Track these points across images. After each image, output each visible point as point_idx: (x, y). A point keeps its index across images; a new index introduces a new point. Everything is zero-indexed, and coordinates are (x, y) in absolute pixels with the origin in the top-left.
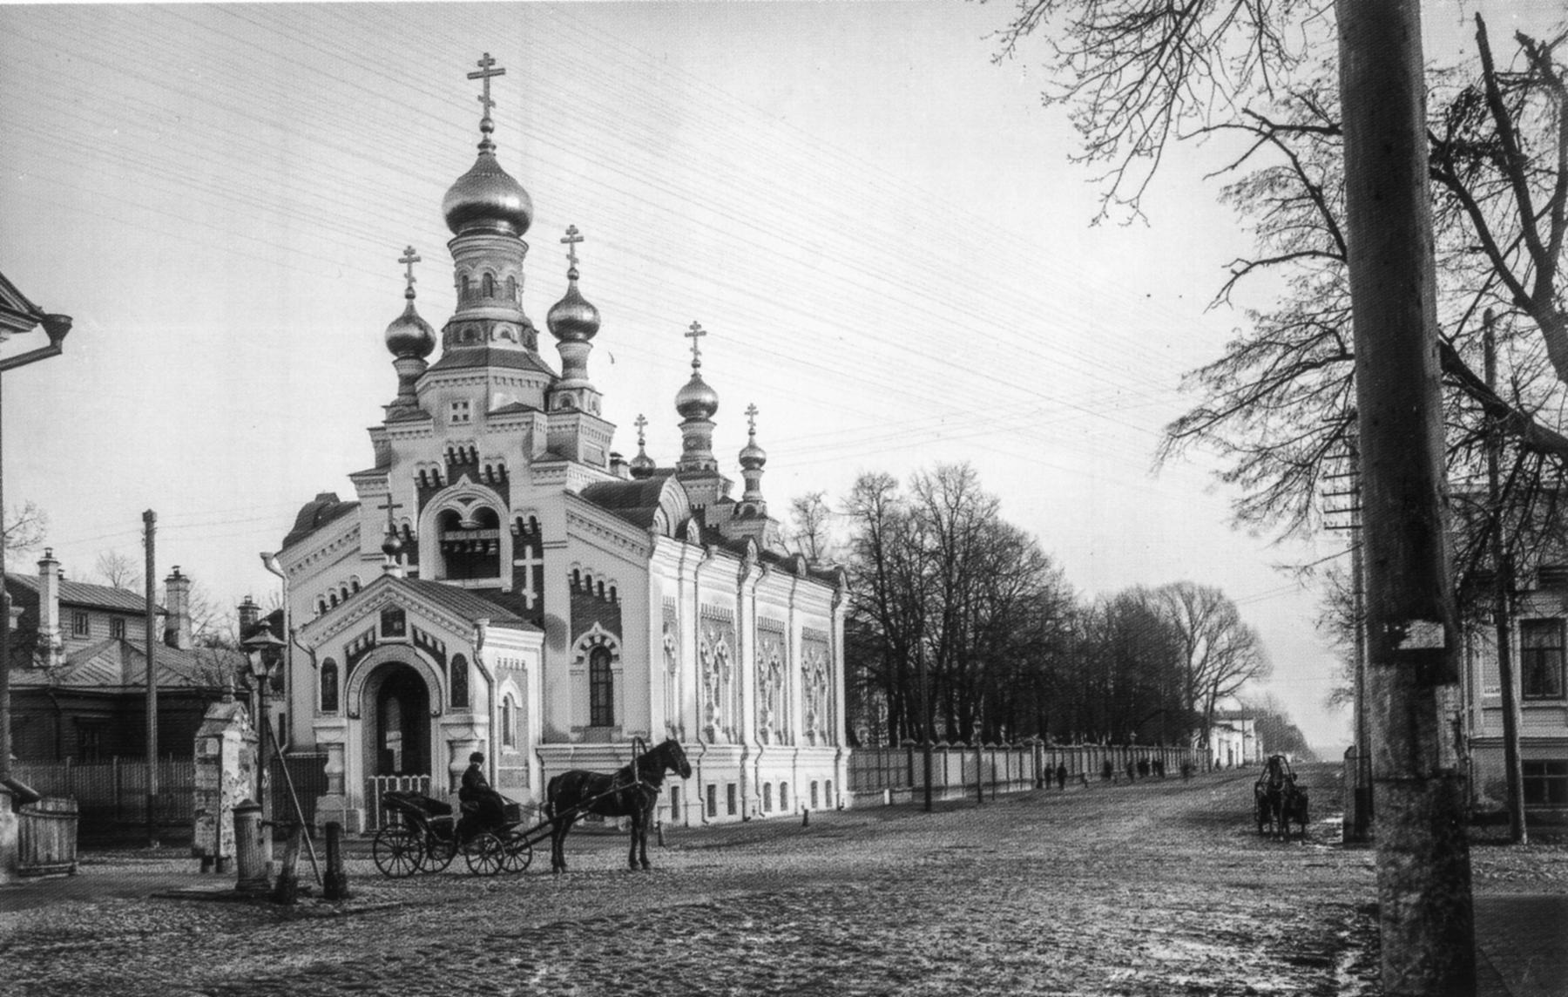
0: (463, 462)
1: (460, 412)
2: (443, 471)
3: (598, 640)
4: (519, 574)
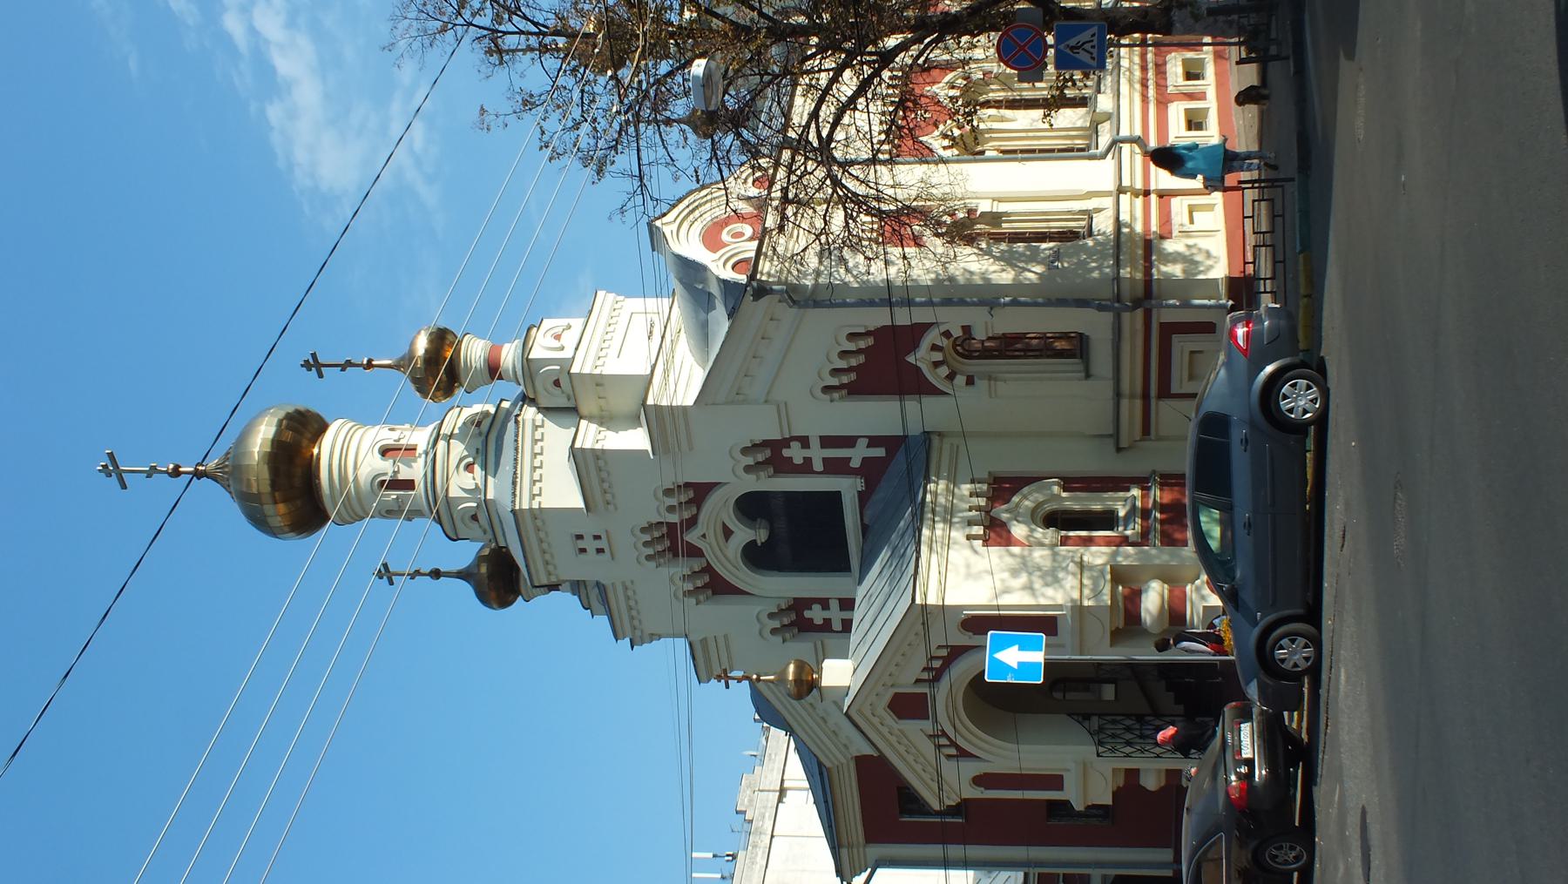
0: (671, 541)
1: (591, 545)
2: (683, 567)
4: (836, 467)
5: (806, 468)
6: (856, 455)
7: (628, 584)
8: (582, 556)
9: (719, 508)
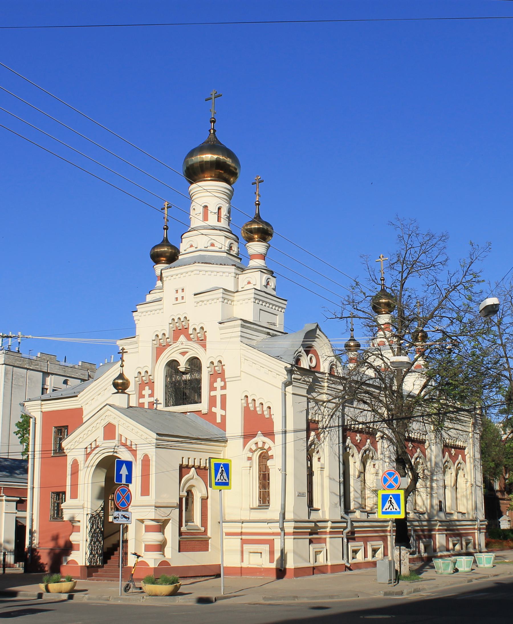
1: (180, 294)
3: (260, 445)
4: (212, 401)
5: (212, 388)
6: (218, 410)
7: (162, 311)
8: (175, 292)
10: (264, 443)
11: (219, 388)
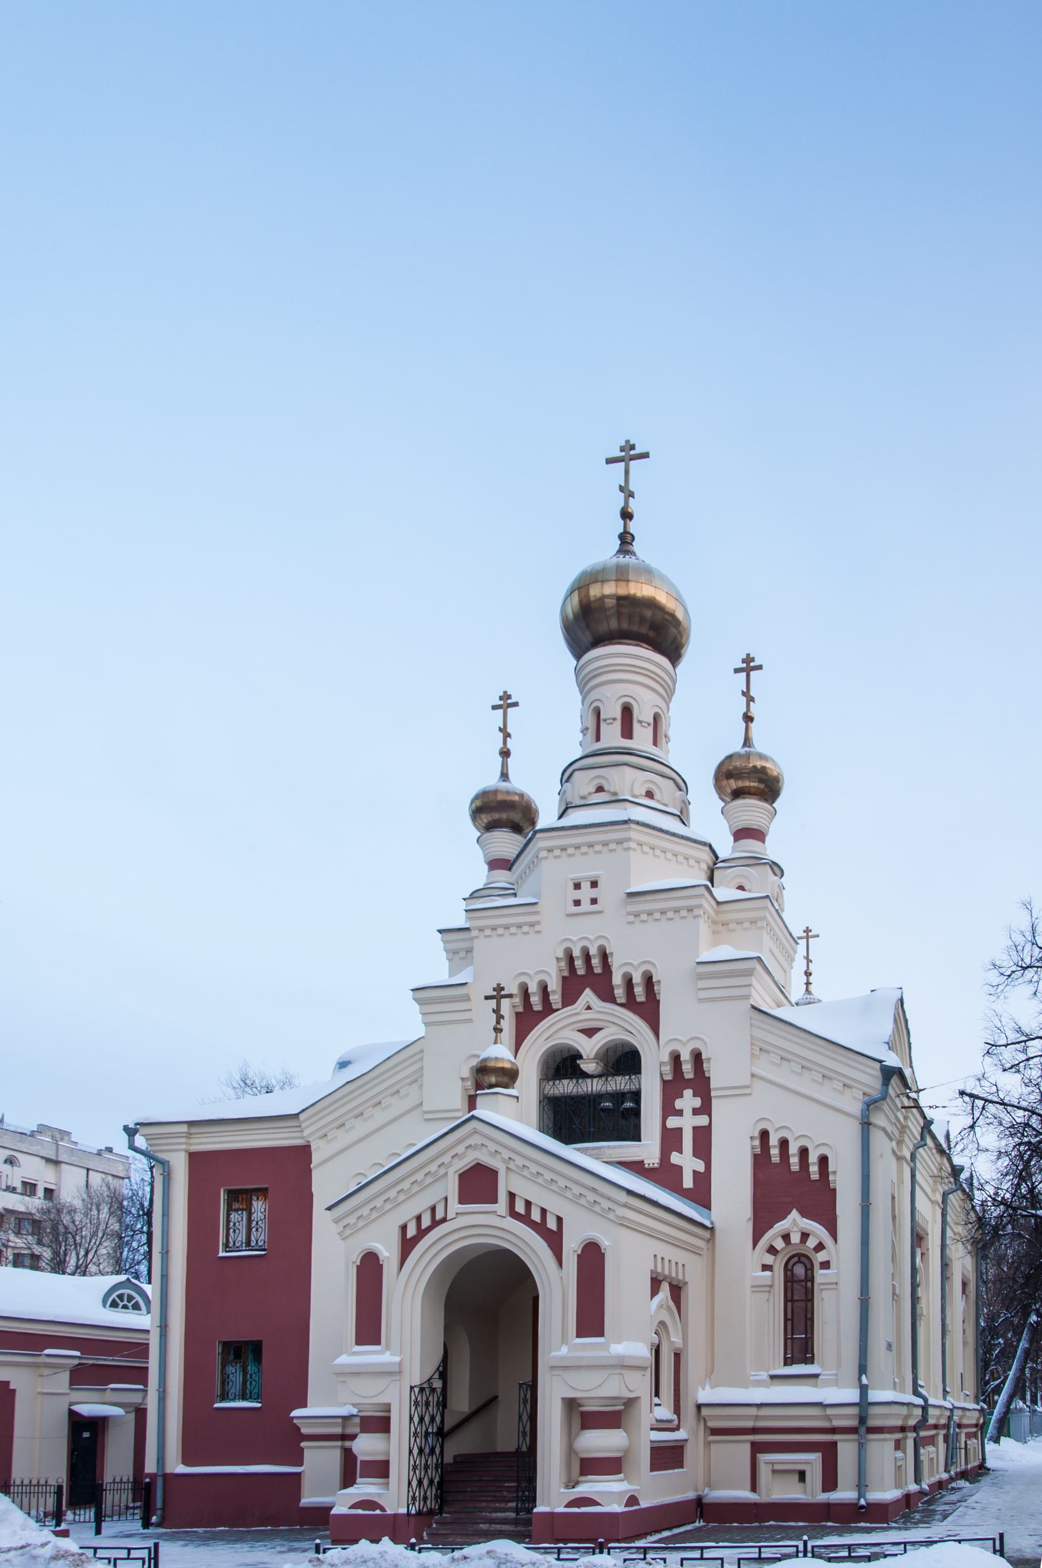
0: (587, 975)
5: (669, 1109)
9: (622, 1026)
10: (805, 1236)
11: (688, 1112)
